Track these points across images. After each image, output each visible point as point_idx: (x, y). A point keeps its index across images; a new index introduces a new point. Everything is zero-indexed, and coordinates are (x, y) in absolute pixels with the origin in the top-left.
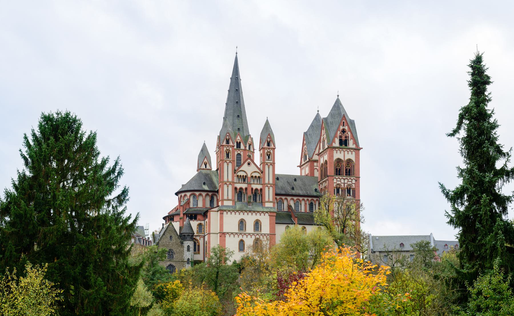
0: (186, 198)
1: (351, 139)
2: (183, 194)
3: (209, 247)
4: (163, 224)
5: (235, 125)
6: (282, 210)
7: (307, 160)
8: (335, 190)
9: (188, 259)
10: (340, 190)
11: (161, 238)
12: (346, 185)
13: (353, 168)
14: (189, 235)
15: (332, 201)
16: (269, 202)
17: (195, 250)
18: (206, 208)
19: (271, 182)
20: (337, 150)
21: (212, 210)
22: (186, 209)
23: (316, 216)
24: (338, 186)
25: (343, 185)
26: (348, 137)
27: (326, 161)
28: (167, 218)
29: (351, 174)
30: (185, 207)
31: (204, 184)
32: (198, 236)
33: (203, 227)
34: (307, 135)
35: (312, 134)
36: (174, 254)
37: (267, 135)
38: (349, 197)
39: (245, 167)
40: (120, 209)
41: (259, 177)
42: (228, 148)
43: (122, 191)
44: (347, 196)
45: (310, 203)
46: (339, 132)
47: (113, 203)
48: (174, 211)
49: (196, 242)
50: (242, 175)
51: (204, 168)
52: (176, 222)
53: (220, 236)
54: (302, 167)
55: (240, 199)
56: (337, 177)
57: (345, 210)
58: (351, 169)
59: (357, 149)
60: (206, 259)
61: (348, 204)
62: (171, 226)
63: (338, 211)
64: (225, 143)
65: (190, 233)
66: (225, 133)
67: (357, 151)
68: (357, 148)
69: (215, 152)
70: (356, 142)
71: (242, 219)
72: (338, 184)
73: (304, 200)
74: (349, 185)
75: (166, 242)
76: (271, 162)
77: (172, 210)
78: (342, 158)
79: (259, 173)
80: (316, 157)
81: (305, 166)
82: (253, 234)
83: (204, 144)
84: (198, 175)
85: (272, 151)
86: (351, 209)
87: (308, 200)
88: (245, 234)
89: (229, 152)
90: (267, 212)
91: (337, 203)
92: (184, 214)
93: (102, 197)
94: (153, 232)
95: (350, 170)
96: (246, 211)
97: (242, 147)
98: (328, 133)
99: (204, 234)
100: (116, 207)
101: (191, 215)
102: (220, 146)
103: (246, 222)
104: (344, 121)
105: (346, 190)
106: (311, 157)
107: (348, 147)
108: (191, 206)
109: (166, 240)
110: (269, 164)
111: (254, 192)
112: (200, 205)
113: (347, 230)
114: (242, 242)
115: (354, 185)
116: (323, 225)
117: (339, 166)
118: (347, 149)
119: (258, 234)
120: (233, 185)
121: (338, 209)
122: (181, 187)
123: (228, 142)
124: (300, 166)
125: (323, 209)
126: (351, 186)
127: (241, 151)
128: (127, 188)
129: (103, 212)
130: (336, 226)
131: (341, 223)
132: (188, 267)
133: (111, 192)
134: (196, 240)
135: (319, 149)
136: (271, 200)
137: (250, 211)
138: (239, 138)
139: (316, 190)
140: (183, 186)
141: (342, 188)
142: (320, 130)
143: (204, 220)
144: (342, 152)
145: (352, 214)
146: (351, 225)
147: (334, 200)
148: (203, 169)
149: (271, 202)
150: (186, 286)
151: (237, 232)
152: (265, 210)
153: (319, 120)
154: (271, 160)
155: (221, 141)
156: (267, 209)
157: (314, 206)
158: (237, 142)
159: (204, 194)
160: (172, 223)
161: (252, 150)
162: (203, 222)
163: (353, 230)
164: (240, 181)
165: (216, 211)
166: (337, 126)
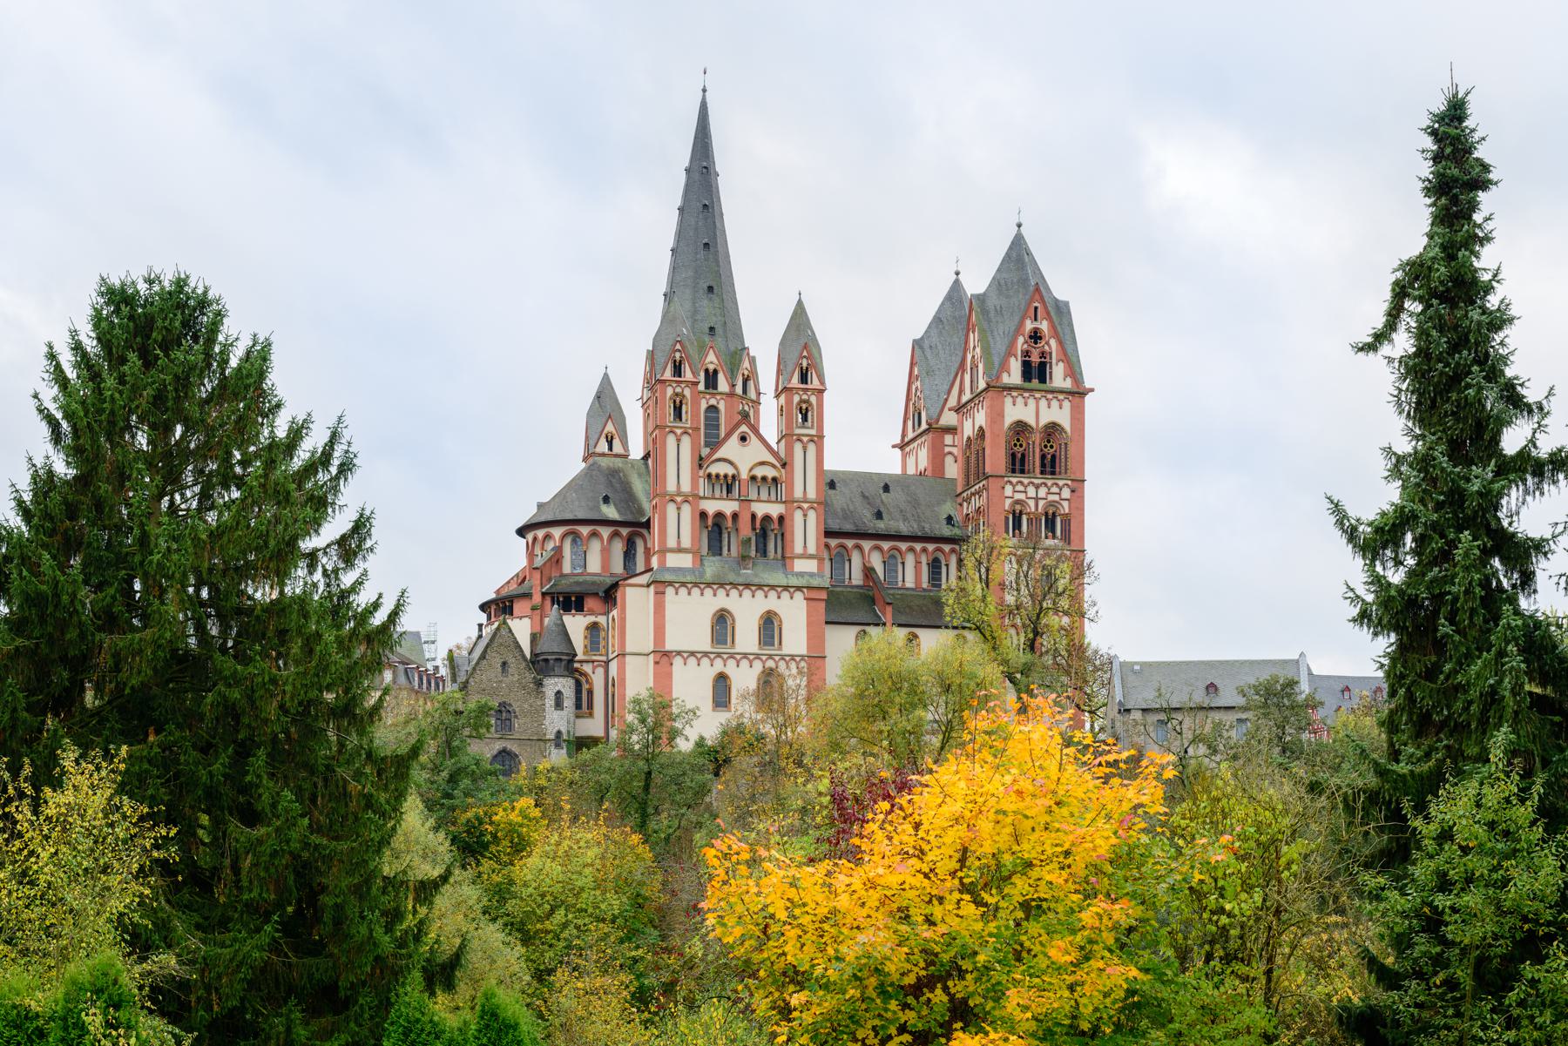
0: (550, 545)
2: (541, 533)
3: (623, 696)
4: (480, 626)
5: (699, 317)
7: (924, 426)
8: (1007, 519)
9: (559, 732)
10: (1024, 518)
11: (474, 669)
12: (1041, 503)
14: (561, 660)
15: (1000, 554)
17: (578, 706)
18: (612, 575)
19: (812, 494)
20: (1015, 394)
22: (550, 580)
23: (951, 602)
24: (1018, 508)
25: (1032, 503)
26: (1051, 353)
27: (981, 428)
28: (493, 607)
30: (546, 572)
31: (606, 500)
32: (587, 662)
33: (602, 634)
34: (921, 348)
35: (940, 347)
36: (516, 717)
37: (799, 348)
38: (1050, 542)
39: (731, 449)
40: (348, 579)
41: (775, 480)
42: (678, 390)
43: (352, 524)
44: (1046, 537)
45: (931, 559)
46: (1021, 340)
47: (324, 560)
48: (514, 586)
49: (583, 680)
50: (722, 473)
51: (606, 449)
52: (521, 618)
53: (656, 663)
54: (907, 449)
55: (715, 547)
56: (1014, 480)
57: (1037, 581)
59: (1078, 394)
60: (614, 734)
61: (1048, 562)
62: (503, 632)
63: (1017, 584)
64: (668, 374)
65: (562, 654)
66: (670, 343)
67: (1077, 400)
68: (1075, 390)
69: (640, 403)
70: (1074, 371)
71: (723, 610)
72: (1018, 502)
73: (911, 549)
74: (1052, 504)
75: (490, 680)
76: (813, 432)
77: (508, 582)
78: (1032, 422)
79: (774, 466)
80: (949, 418)
81: (915, 444)
82: (758, 656)
83: (606, 376)
84: (586, 474)
85: (813, 399)
86: (1056, 580)
87: (924, 550)
88: (732, 656)
90: (799, 588)
91: (1013, 559)
92: (544, 595)
93: (292, 543)
94: (450, 651)
95: (1054, 457)
96: (734, 585)
97: (723, 385)
98: (988, 342)
99: (607, 655)
100: (336, 571)
102: (653, 383)
104: (1036, 304)
106: (935, 416)
107: (1048, 385)
108: (567, 568)
109: (491, 673)
112: (594, 565)
113: (1045, 642)
114: (722, 680)
115: (1065, 504)
116: (970, 629)
118: (1046, 391)
119: (770, 657)
121: (1018, 577)
122: (535, 511)
123: (678, 371)
124: (902, 446)
125: (973, 580)
128: (367, 513)
129: (294, 588)
130: (1012, 631)
131: (1027, 622)
132: (558, 757)
133: (319, 525)
134: (581, 674)
135: (961, 391)
136: (812, 549)
137: (747, 586)
138: (711, 357)
139: (949, 519)
140: (540, 506)
141: (1028, 514)
142: (962, 334)
143: (606, 613)
144: (1031, 402)
145: (1060, 595)
146: (1057, 627)
147: (1007, 550)
148: (603, 455)
149: (811, 557)
150: (551, 816)
151: (708, 648)
152: (794, 581)
153: (961, 302)
154: (812, 427)
155: (658, 368)
157: (944, 569)
158: (707, 371)
159: (605, 532)
160: (509, 621)
161: (753, 395)
162: (602, 620)
163: (1064, 642)
164: (717, 495)
165: (642, 586)
166: (1017, 319)
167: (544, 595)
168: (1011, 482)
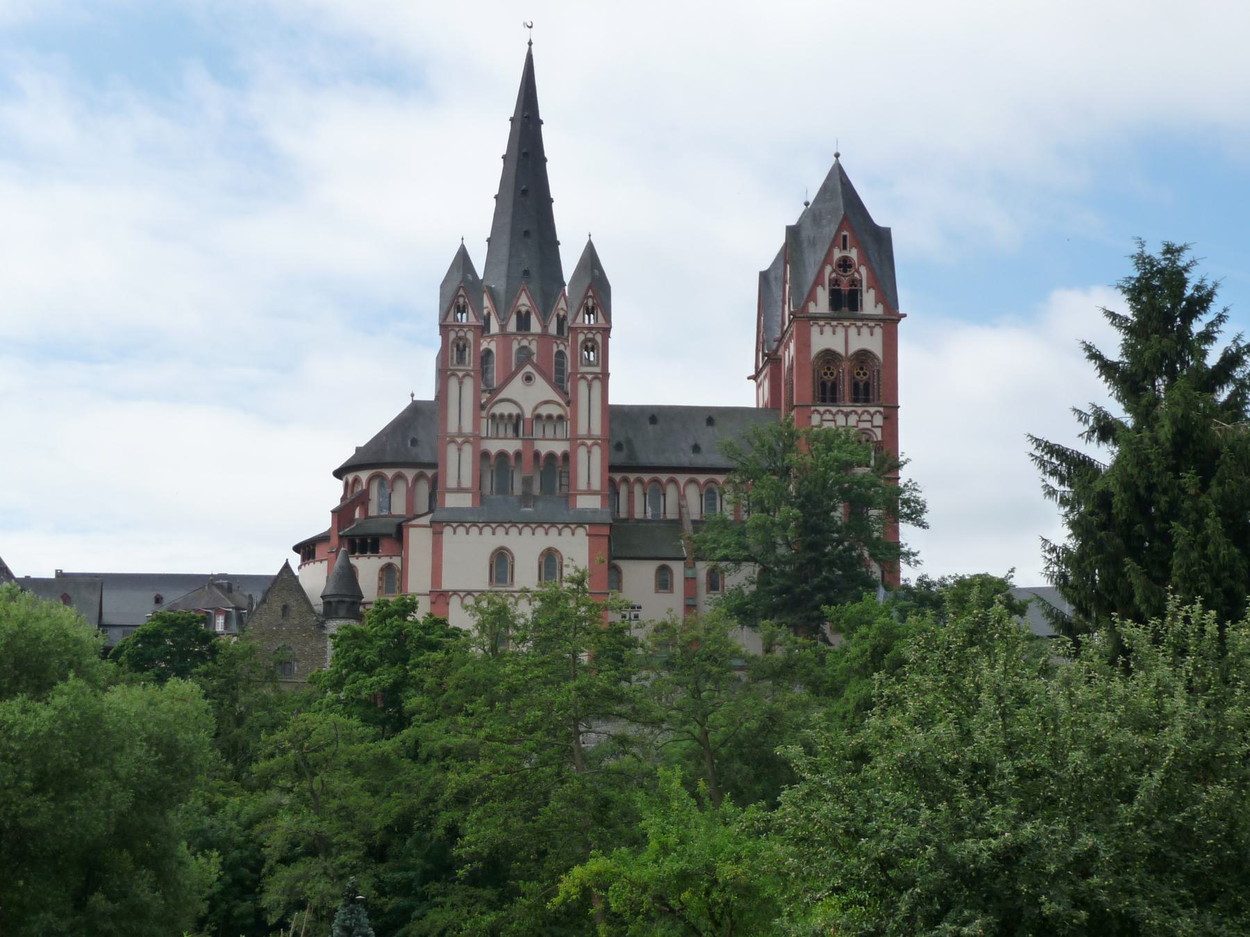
6: (662, 515)
13: (876, 377)
16: (590, 492)
20: (822, 323)
21: (414, 522)
29: (871, 397)
41: (560, 418)
46: (828, 269)
50: (506, 413)
52: (321, 561)
55: (503, 487)
56: (822, 409)
58: (871, 383)
59: (890, 321)
65: (345, 596)
70: (888, 296)
71: (502, 548)
74: (864, 431)
76: (598, 370)
78: (840, 349)
79: (559, 405)
85: (599, 338)
89: (465, 346)
90: (580, 525)
95: (867, 385)
101: (363, 539)
103: (513, 558)
104: (845, 233)
108: (373, 511)
110: (590, 377)
111: (542, 462)
112: (399, 507)
115: (878, 432)
117: (832, 374)
120: (475, 446)
126: (871, 436)
127: (530, 338)
144: (840, 331)
154: (597, 365)
162: (396, 561)
166: (827, 247)
168: (818, 412)
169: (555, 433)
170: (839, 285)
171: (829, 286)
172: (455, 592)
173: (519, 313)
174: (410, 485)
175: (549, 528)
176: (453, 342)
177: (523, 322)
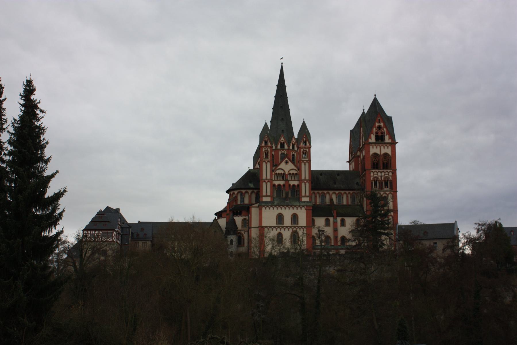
1: (387, 134)
6: (325, 203)
8: (372, 183)
12: (383, 177)
13: (389, 162)
16: (305, 196)
20: (373, 145)
21: (253, 206)
24: (376, 179)
25: (380, 178)
26: (384, 132)
29: (388, 167)
31: (250, 182)
32: (242, 230)
41: (296, 174)
42: (266, 149)
44: (385, 188)
46: (374, 129)
52: (224, 218)
59: (393, 143)
71: (280, 213)
72: (376, 177)
74: (386, 177)
76: (307, 159)
78: (379, 153)
79: (296, 170)
82: (291, 227)
85: (307, 150)
88: (283, 227)
89: (267, 153)
90: (303, 206)
95: (387, 163)
104: (379, 118)
105: (384, 182)
108: (239, 203)
110: (305, 162)
111: (291, 188)
112: (246, 201)
115: (391, 177)
117: (376, 160)
118: (383, 144)
119: (295, 227)
120: (271, 183)
127: (284, 150)
141: (379, 181)
144: (378, 147)
152: (302, 204)
154: (307, 158)
156: (304, 203)
162: (247, 217)
164: (279, 179)
167: (230, 210)
168: (373, 172)
169: (295, 178)
170: (378, 134)
171: (375, 134)
172: (266, 227)
173: (281, 143)
174: (250, 195)
175: (294, 207)
176: (264, 152)
177: (282, 146)
